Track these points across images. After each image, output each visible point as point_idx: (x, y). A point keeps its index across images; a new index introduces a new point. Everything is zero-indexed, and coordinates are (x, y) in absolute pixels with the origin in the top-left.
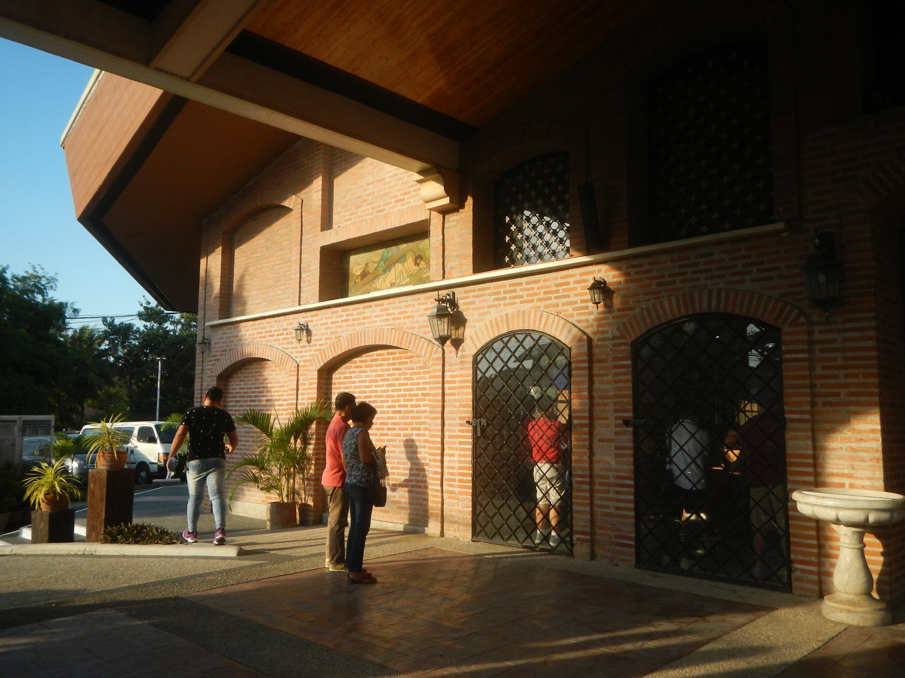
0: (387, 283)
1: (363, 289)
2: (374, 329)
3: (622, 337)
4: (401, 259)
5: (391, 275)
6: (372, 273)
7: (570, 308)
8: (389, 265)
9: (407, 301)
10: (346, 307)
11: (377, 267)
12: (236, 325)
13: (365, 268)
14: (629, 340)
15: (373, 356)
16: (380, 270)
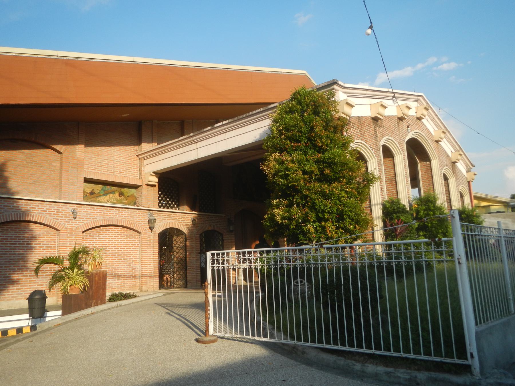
0: (105, 200)
1: (92, 199)
2: (117, 219)
3: (198, 233)
4: (113, 192)
5: (107, 197)
6: (97, 194)
7: (185, 224)
8: (106, 193)
9: (131, 211)
10: (99, 207)
11: (99, 192)
12: (8, 200)
13: (92, 191)
14: (199, 234)
15: (107, 228)
16: (102, 194)
